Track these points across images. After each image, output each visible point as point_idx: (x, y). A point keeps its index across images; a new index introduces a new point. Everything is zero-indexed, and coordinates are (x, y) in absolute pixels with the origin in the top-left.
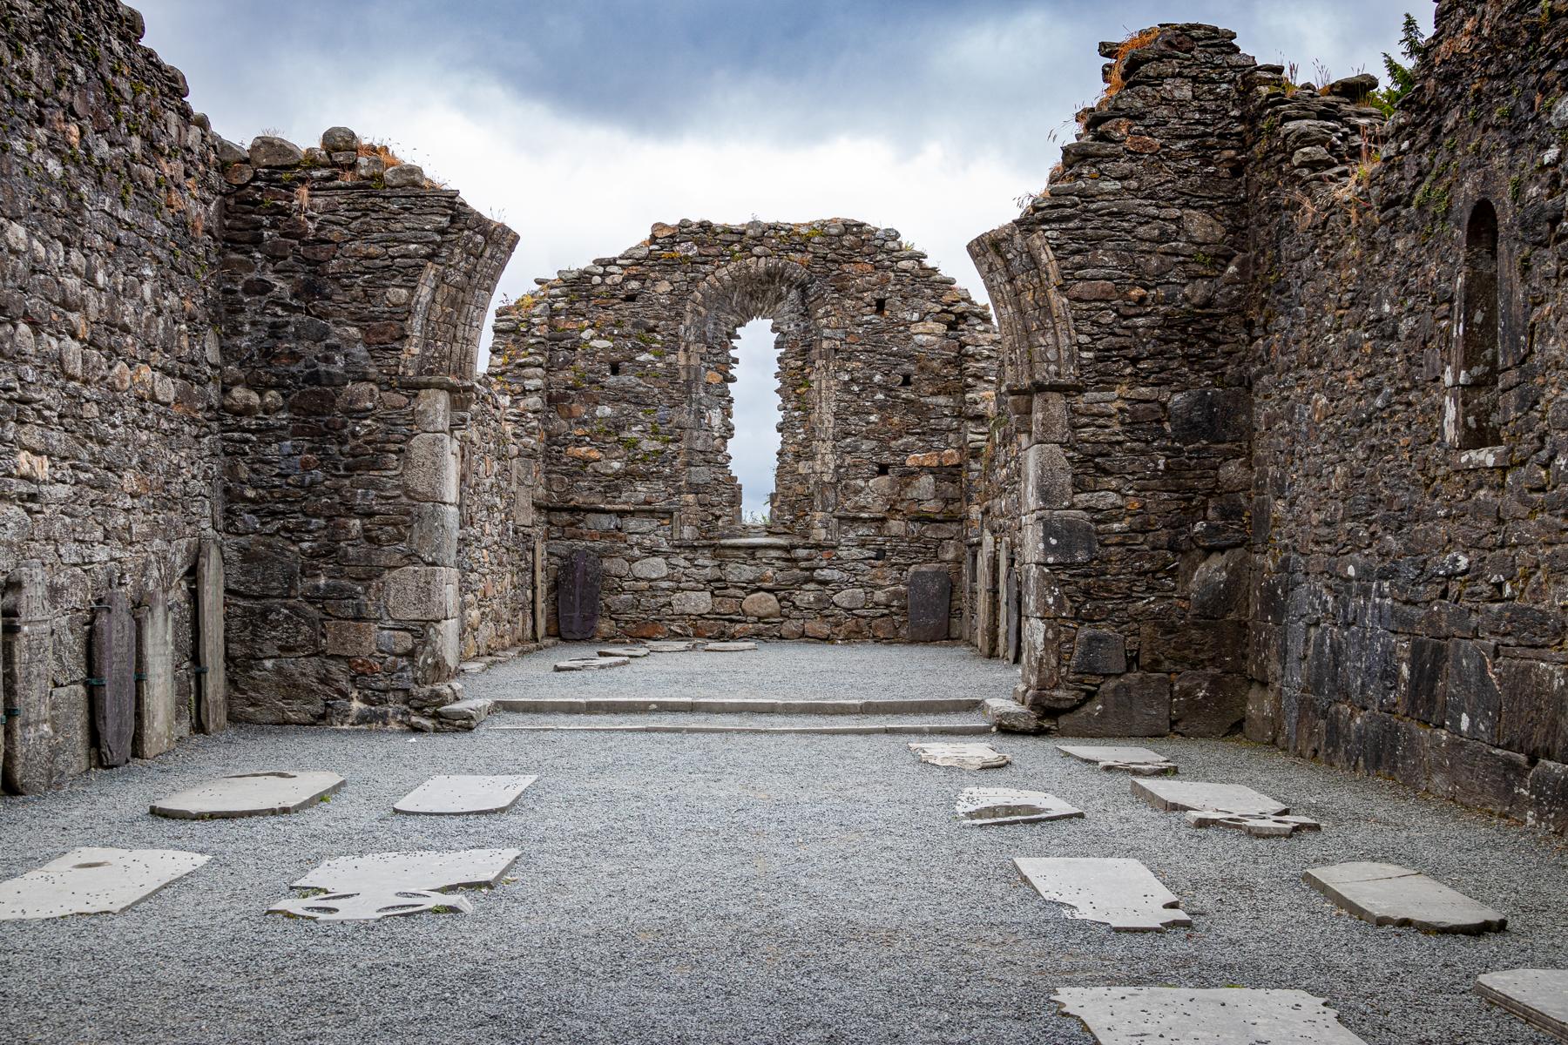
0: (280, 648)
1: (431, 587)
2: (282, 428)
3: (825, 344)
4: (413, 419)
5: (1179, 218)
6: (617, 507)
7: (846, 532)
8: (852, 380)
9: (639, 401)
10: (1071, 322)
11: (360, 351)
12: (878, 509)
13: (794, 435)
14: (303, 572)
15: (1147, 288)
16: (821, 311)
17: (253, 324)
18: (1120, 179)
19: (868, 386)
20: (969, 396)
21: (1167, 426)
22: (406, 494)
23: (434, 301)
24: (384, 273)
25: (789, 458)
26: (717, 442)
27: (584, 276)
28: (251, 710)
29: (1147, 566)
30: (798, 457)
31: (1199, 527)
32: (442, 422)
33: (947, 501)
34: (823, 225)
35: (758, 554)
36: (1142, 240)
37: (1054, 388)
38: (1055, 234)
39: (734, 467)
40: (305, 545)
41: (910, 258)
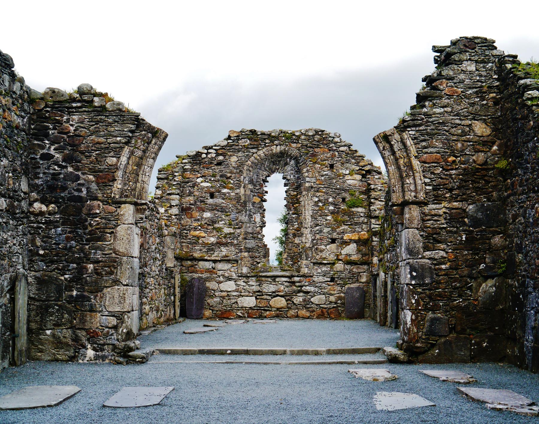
0: (54, 325)
1: (126, 296)
2: (57, 222)
3: (307, 185)
4: (118, 218)
5: (470, 125)
6: (213, 258)
7: (317, 269)
8: (319, 201)
9: (223, 210)
10: (421, 172)
11: (94, 186)
12: (332, 257)
13: (293, 226)
14: (65, 289)
15: (456, 157)
16: (305, 170)
17: (44, 173)
18: (443, 107)
19: (326, 203)
20: (371, 208)
21: (466, 220)
22: (115, 252)
23: (128, 163)
24: (105, 150)
25: (291, 236)
26: (258, 229)
27: (199, 154)
28: (39, 354)
29: (458, 285)
30: (295, 236)
31: (482, 266)
32: (131, 220)
33: (364, 255)
34: (307, 131)
35: (277, 279)
36: (453, 135)
37: (414, 203)
38: (413, 133)
39: (266, 240)
40: (66, 276)
41: (345, 146)
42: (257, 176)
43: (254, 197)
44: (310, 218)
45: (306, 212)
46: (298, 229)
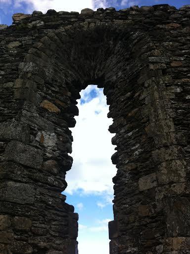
30: (136, 174)
42: (55, 70)
43: (46, 101)
44: (171, 124)
45: (160, 111)
46: (146, 156)
